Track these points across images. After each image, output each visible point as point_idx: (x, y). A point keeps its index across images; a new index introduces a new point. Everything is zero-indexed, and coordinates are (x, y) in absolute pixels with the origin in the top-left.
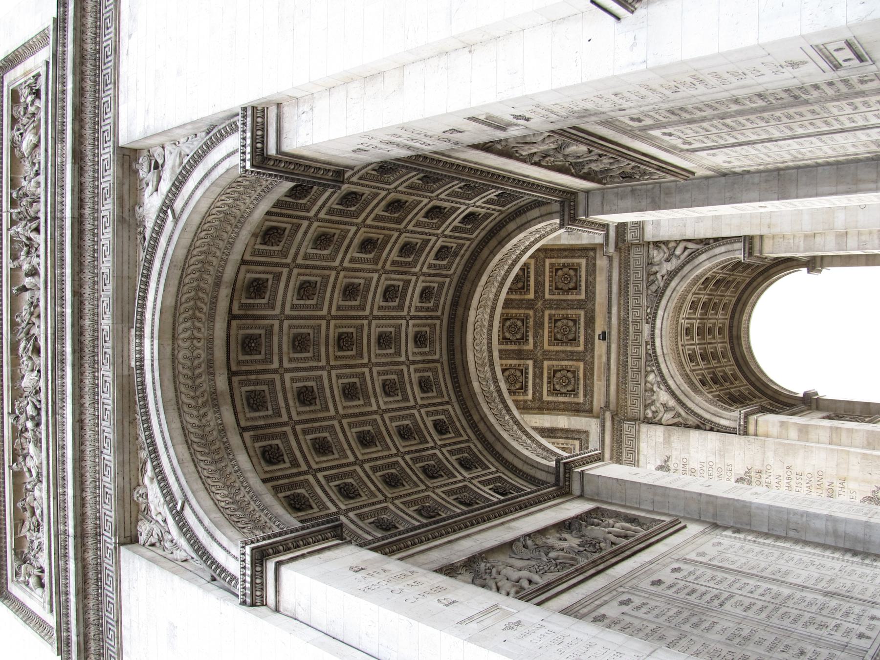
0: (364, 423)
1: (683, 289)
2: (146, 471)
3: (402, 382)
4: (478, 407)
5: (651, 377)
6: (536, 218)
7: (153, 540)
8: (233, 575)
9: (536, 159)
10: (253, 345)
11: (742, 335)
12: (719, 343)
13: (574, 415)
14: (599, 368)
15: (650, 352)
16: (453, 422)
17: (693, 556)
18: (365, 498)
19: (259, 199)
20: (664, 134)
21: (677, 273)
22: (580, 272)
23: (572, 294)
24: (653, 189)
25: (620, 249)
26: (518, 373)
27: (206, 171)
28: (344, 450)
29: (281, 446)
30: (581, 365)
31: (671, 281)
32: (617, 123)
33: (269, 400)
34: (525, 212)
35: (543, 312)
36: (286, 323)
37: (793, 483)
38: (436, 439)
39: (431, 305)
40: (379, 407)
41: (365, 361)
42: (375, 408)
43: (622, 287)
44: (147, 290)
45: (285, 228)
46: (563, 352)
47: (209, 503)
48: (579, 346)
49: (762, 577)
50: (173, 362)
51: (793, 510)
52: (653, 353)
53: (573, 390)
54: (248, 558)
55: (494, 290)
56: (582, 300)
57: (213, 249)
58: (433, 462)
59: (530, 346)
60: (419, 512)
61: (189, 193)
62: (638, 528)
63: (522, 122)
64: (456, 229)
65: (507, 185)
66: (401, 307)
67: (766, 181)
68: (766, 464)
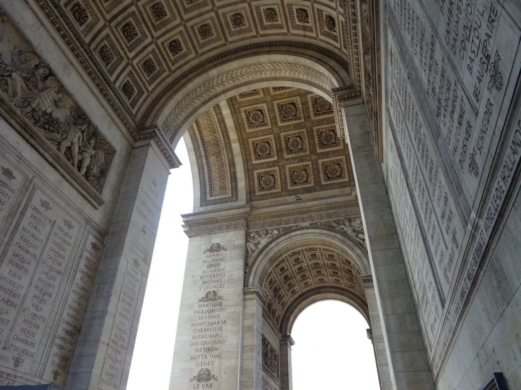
5: (276, 232)
6: (339, 76)
11: (322, 295)
12: (313, 280)
15: (292, 229)
26: (268, 152)
30: (279, 190)
35: (309, 161)
37: (215, 326)
38: (162, 39)
39: (266, 23)
46: (286, 178)
48: (291, 186)
51: (113, 286)
53: (263, 188)
55: (287, 75)
59: (286, 156)
68: (226, 308)
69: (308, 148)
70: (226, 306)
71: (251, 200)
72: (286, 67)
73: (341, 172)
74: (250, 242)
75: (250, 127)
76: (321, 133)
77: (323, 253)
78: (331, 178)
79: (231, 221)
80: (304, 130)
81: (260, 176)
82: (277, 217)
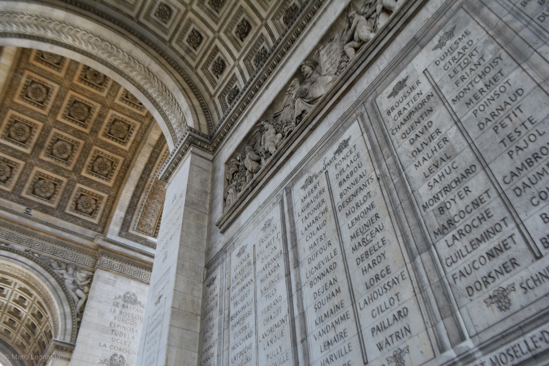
9: (307, 69)
20: (345, 143)
21: (61, 286)
23: (72, 204)
24: (205, 208)
25: (97, 250)
26: (23, 138)
30: (9, 189)
31: (56, 279)
32: (391, 76)
34: (205, 115)
35: (67, 177)
46: (26, 181)
48: (27, 193)
55: (138, 79)
59: (42, 156)
65: (264, 70)
67: (193, 302)
72: (143, 72)
75: (22, 97)
76: (99, 157)
77: (15, 292)
80: (82, 142)
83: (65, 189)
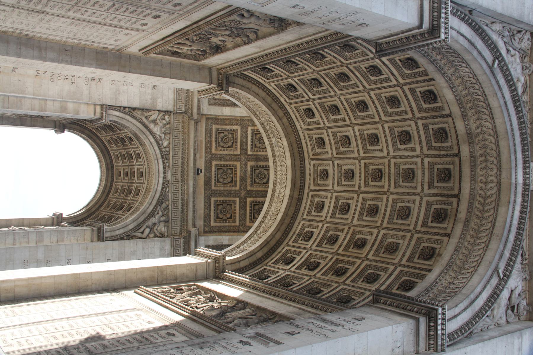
0: (363, 117)
1: (145, 205)
2: (523, 86)
3: (337, 145)
4: (283, 127)
5: (166, 143)
7: (519, 35)
8: (455, 16)
10: (443, 176)
12: (120, 166)
13: (219, 116)
14: (201, 149)
15: (166, 161)
16: (301, 117)
17: (134, 33)
18: (362, 66)
19: (435, 283)
21: (148, 216)
22: (215, 216)
23: (220, 201)
25: (187, 233)
27: (473, 306)
28: (378, 99)
29: (423, 103)
30: (214, 151)
31: (153, 210)
32: (184, 332)
33: (432, 135)
34: (250, 264)
36: (419, 190)
38: (313, 106)
39: (317, 199)
40: (353, 129)
41: (363, 162)
42: (356, 128)
43: (185, 206)
44: (520, 219)
45: (418, 259)
46: (227, 160)
47: (474, 66)
48: (216, 165)
49: (87, 22)
50: (500, 166)
51: (68, 64)
52: (164, 161)
54: (443, 30)
55: (272, 209)
56: (213, 197)
57: (470, 247)
58: (315, 89)
59: (250, 164)
60: (324, 57)
61: (486, 289)
62: (170, 49)
63: (245, 340)
64: (299, 253)
66: (337, 199)
69: (254, 189)
70: (90, 85)
71: (207, 119)
72: (276, 210)
73: (222, 218)
74: (159, 115)
77: (142, 185)
78: (217, 207)
79: (186, 96)
81: (234, 132)
82: (182, 146)
83: (232, 190)
